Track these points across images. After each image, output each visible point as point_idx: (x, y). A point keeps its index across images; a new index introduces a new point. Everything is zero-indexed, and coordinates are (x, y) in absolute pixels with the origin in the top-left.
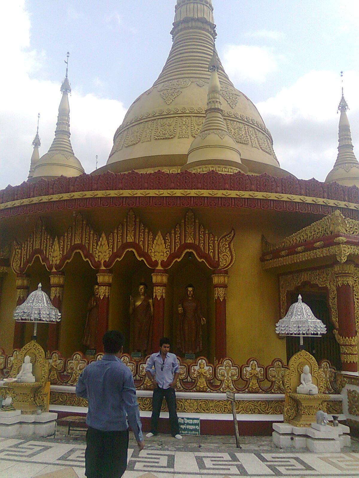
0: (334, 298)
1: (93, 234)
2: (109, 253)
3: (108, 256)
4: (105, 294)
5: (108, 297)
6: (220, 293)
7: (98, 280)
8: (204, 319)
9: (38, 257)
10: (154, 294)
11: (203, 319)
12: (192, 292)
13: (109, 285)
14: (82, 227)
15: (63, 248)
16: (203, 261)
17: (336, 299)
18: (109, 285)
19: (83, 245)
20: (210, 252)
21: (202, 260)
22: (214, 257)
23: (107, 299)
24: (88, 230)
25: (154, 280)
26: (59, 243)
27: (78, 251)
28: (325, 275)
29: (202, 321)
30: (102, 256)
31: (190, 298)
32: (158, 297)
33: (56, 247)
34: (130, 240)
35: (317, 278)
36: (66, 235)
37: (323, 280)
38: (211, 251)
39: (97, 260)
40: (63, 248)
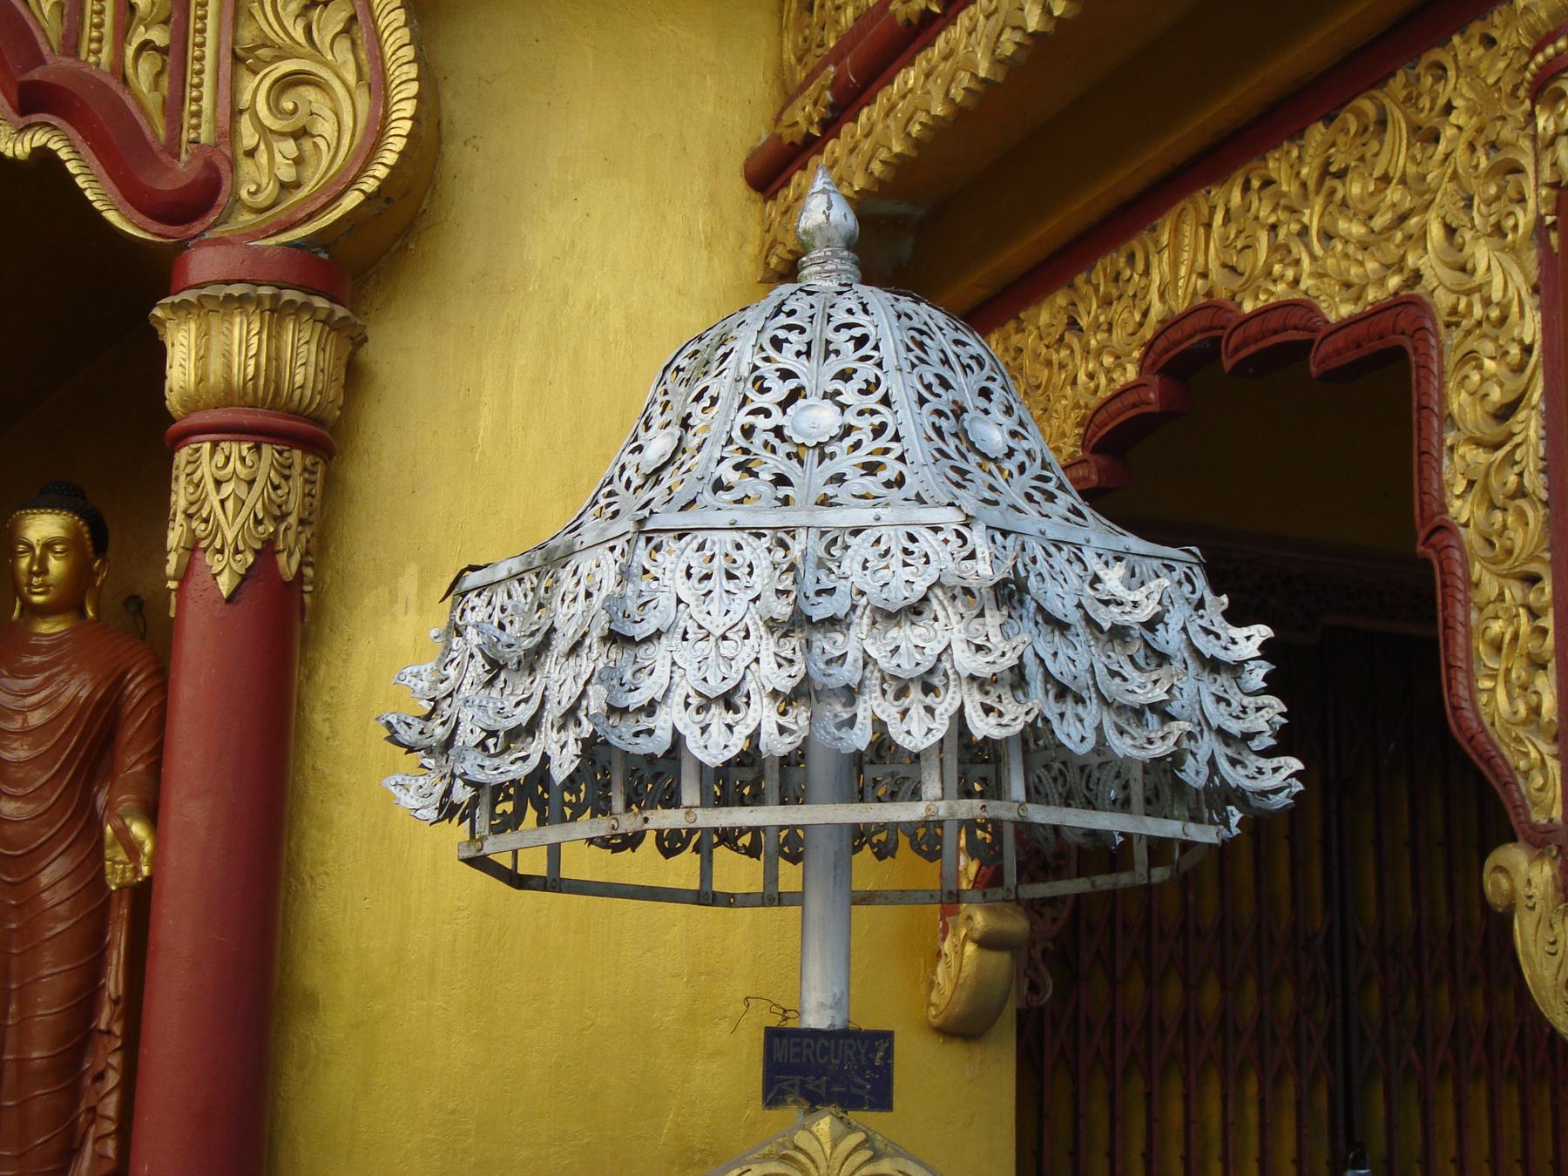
0: (1506, 412)
6: (217, 500)
8: (138, 830)
11: (123, 835)
12: (55, 565)
16: (43, 155)
17: (1530, 426)
20: (130, 52)
21: (40, 138)
22: (174, 107)
28: (1396, 153)
29: (115, 855)
31: (48, 628)
35: (1304, 231)
37: (1379, 222)
38: (139, 35)
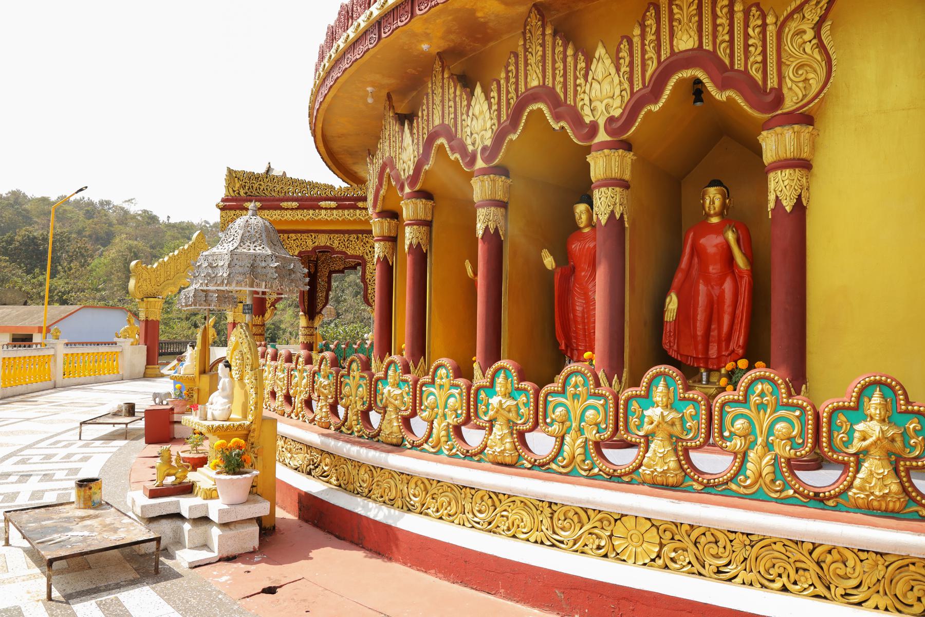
1: (575, 56)
2: (622, 97)
3: (617, 102)
4: (612, 212)
5: (622, 215)
7: (592, 174)
9: (442, 145)
10: (772, 197)
13: (623, 184)
14: (543, 45)
15: (499, 110)
18: (623, 184)
19: (548, 87)
23: (616, 224)
24: (559, 49)
25: (769, 155)
26: (488, 98)
27: (535, 107)
30: (601, 107)
32: (784, 203)
33: (479, 104)
34: (685, 42)
36: (503, 75)
39: (587, 120)
40: (499, 110)
